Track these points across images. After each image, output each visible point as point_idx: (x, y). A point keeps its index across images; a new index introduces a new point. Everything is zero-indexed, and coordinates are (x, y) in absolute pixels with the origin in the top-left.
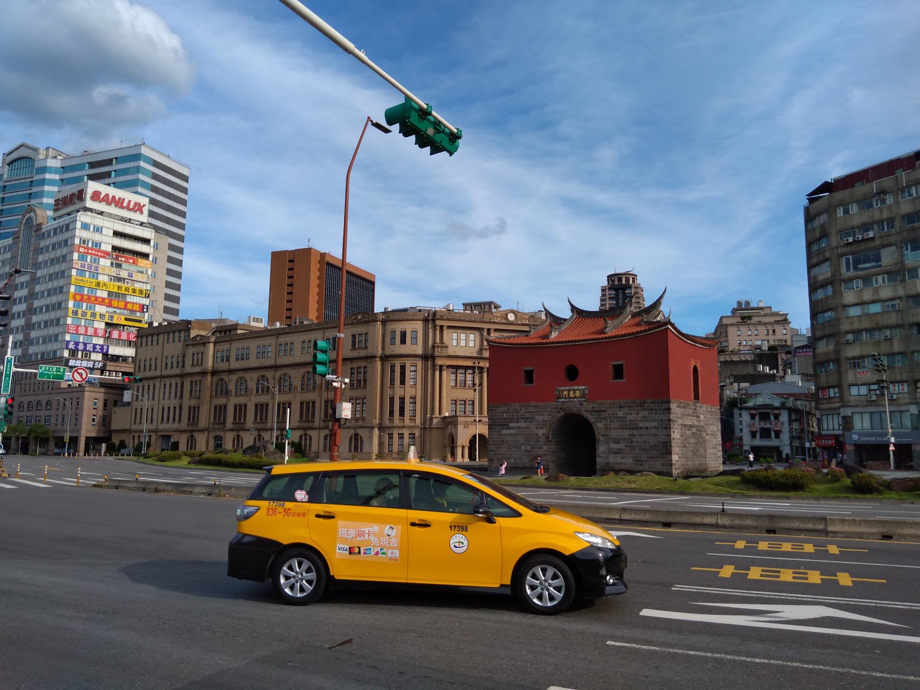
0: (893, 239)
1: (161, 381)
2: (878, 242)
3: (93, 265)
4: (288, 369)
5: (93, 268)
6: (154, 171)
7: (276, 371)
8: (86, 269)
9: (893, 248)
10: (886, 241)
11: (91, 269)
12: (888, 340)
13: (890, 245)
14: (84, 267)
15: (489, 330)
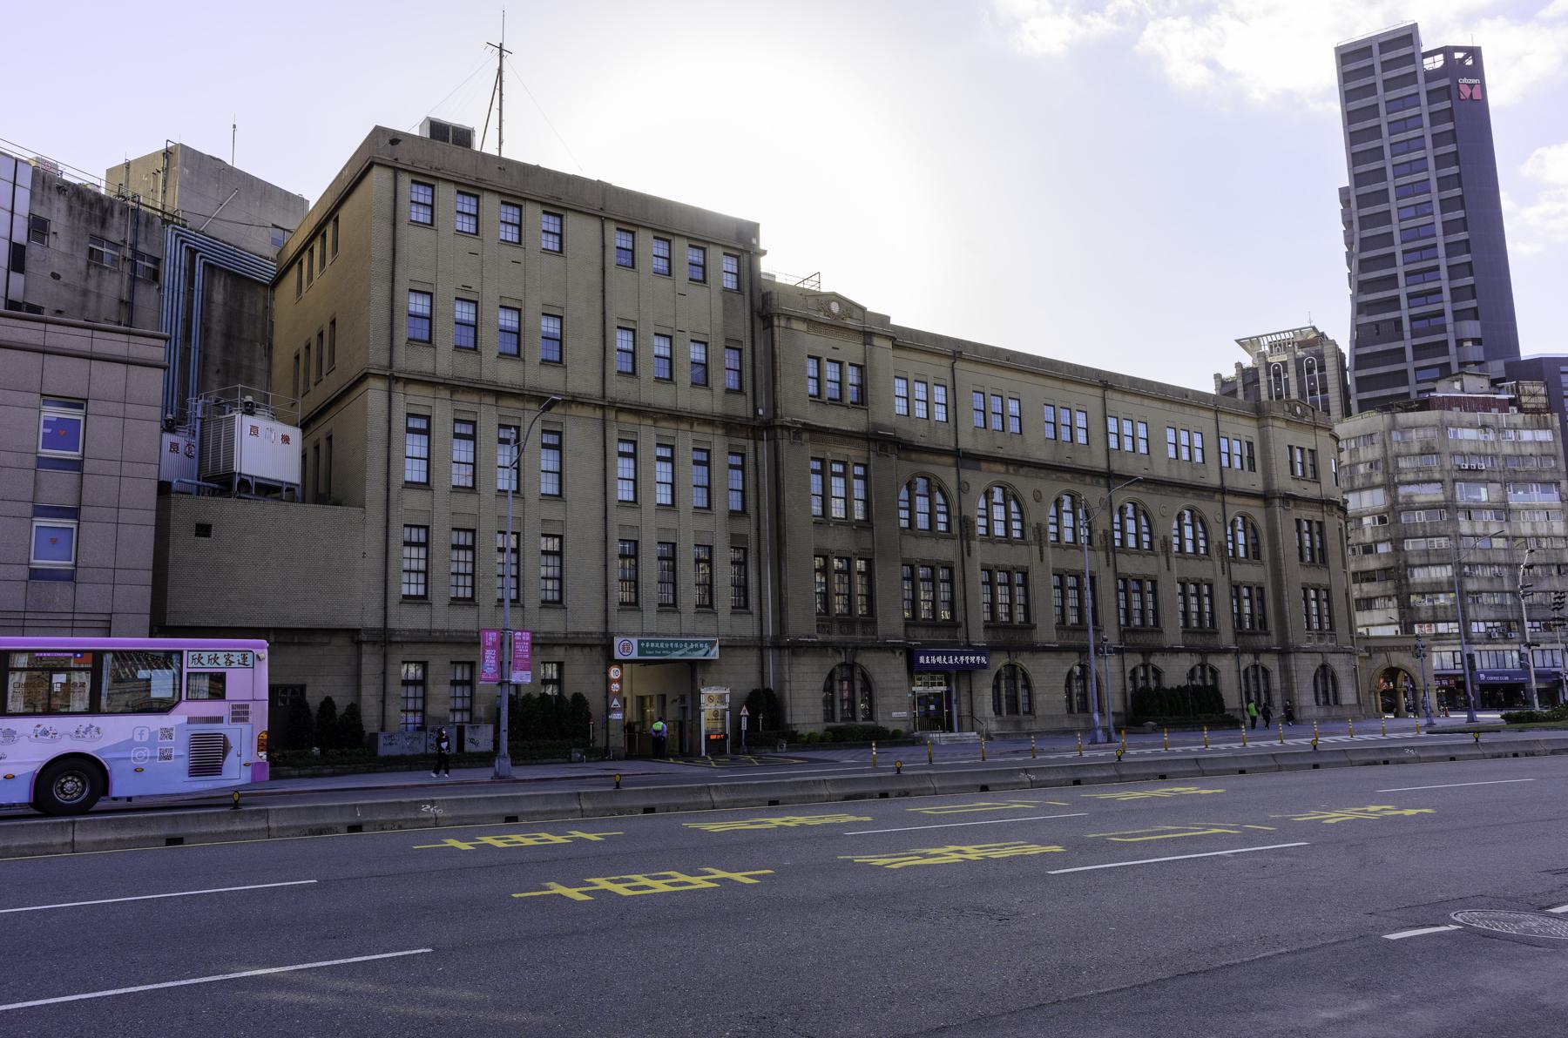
0: (1497, 476)
1: (604, 420)
2: (1484, 476)
4: (1141, 489)
9: (1499, 485)
10: (1491, 476)
12: (1499, 577)
13: (1496, 482)
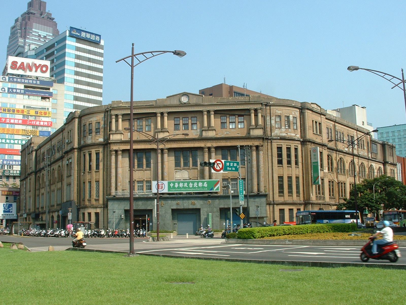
3: (11, 110)
5: (11, 111)
6: (77, 46)
7: (51, 167)
8: (6, 112)
11: (10, 112)
14: (5, 111)
15: (162, 114)
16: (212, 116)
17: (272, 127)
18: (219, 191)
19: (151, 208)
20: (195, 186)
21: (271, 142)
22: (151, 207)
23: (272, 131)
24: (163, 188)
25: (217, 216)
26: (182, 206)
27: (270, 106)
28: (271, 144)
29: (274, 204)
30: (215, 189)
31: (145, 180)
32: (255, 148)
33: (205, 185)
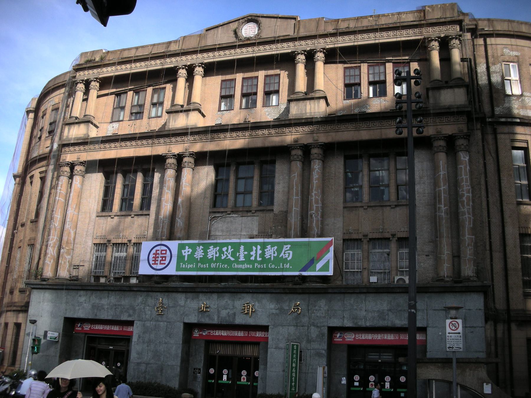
16: (320, 66)
17: (493, 91)
18: (330, 273)
19: (130, 319)
20: (253, 258)
21: (495, 133)
22: (130, 316)
23: (495, 103)
24: (167, 262)
25: (319, 354)
26: (216, 318)
27: (486, 36)
28: (496, 139)
29: (508, 321)
30: (319, 265)
31: (133, 241)
32: (442, 143)
33: (288, 254)
